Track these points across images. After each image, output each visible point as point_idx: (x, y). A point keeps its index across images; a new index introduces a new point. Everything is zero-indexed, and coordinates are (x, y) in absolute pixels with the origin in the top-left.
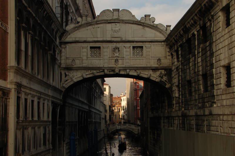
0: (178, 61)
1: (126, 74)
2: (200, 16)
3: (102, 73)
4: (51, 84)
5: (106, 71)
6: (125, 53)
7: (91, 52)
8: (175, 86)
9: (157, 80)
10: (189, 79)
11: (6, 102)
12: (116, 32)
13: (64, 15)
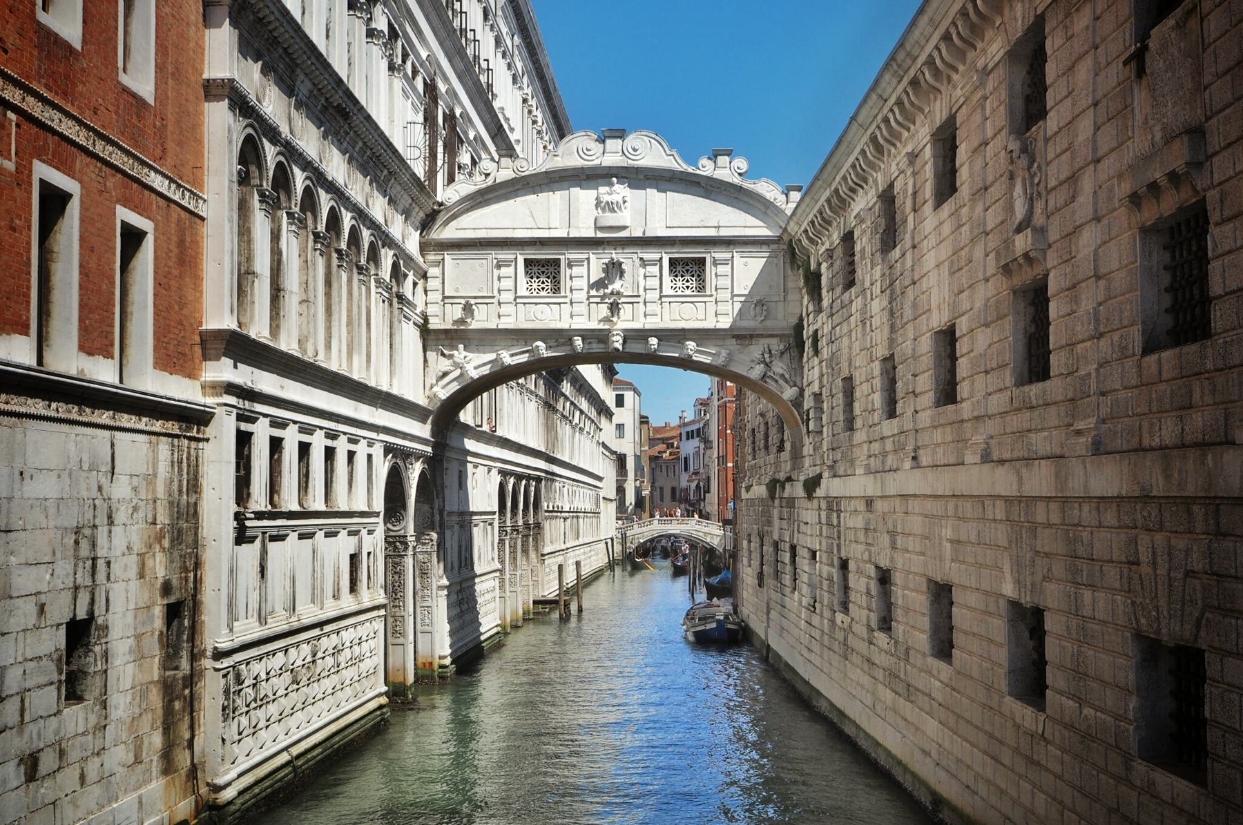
2: (874, 157)
4: (385, 388)
5: (578, 342)
11: (192, 451)
12: (615, 212)
13: (440, 149)
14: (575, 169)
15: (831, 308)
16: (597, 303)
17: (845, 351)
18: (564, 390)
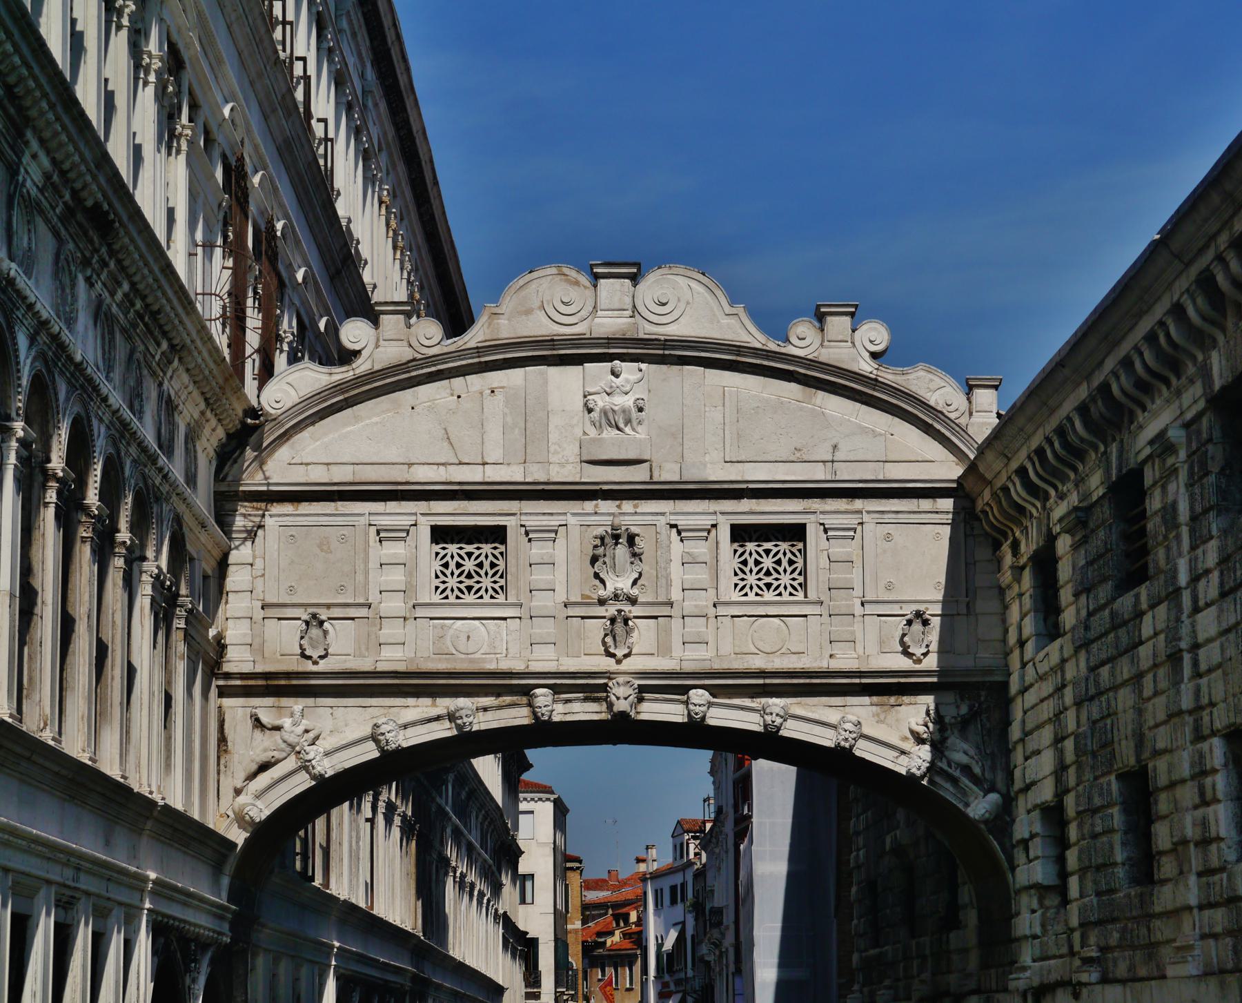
0: (1051, 631)
2: (1204, 318)
3: (518, 716)
5: (543, 697)
6: (676, 571)
7: (437, 566)
8: (1035, 807)
9: (901, 766)
10: (1132, 761)
12: (619, 429)
15: (1087, 628)
16: (583, 618)
17: (1126, 721)
18: (443, 802)
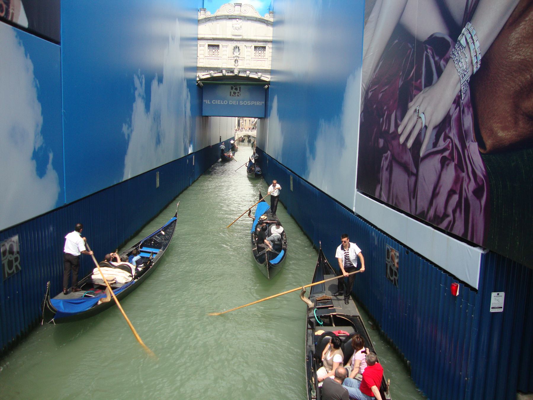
1: (246, 76)
3: (220, 75)
5: (224, 72)
14: (225, 16)
